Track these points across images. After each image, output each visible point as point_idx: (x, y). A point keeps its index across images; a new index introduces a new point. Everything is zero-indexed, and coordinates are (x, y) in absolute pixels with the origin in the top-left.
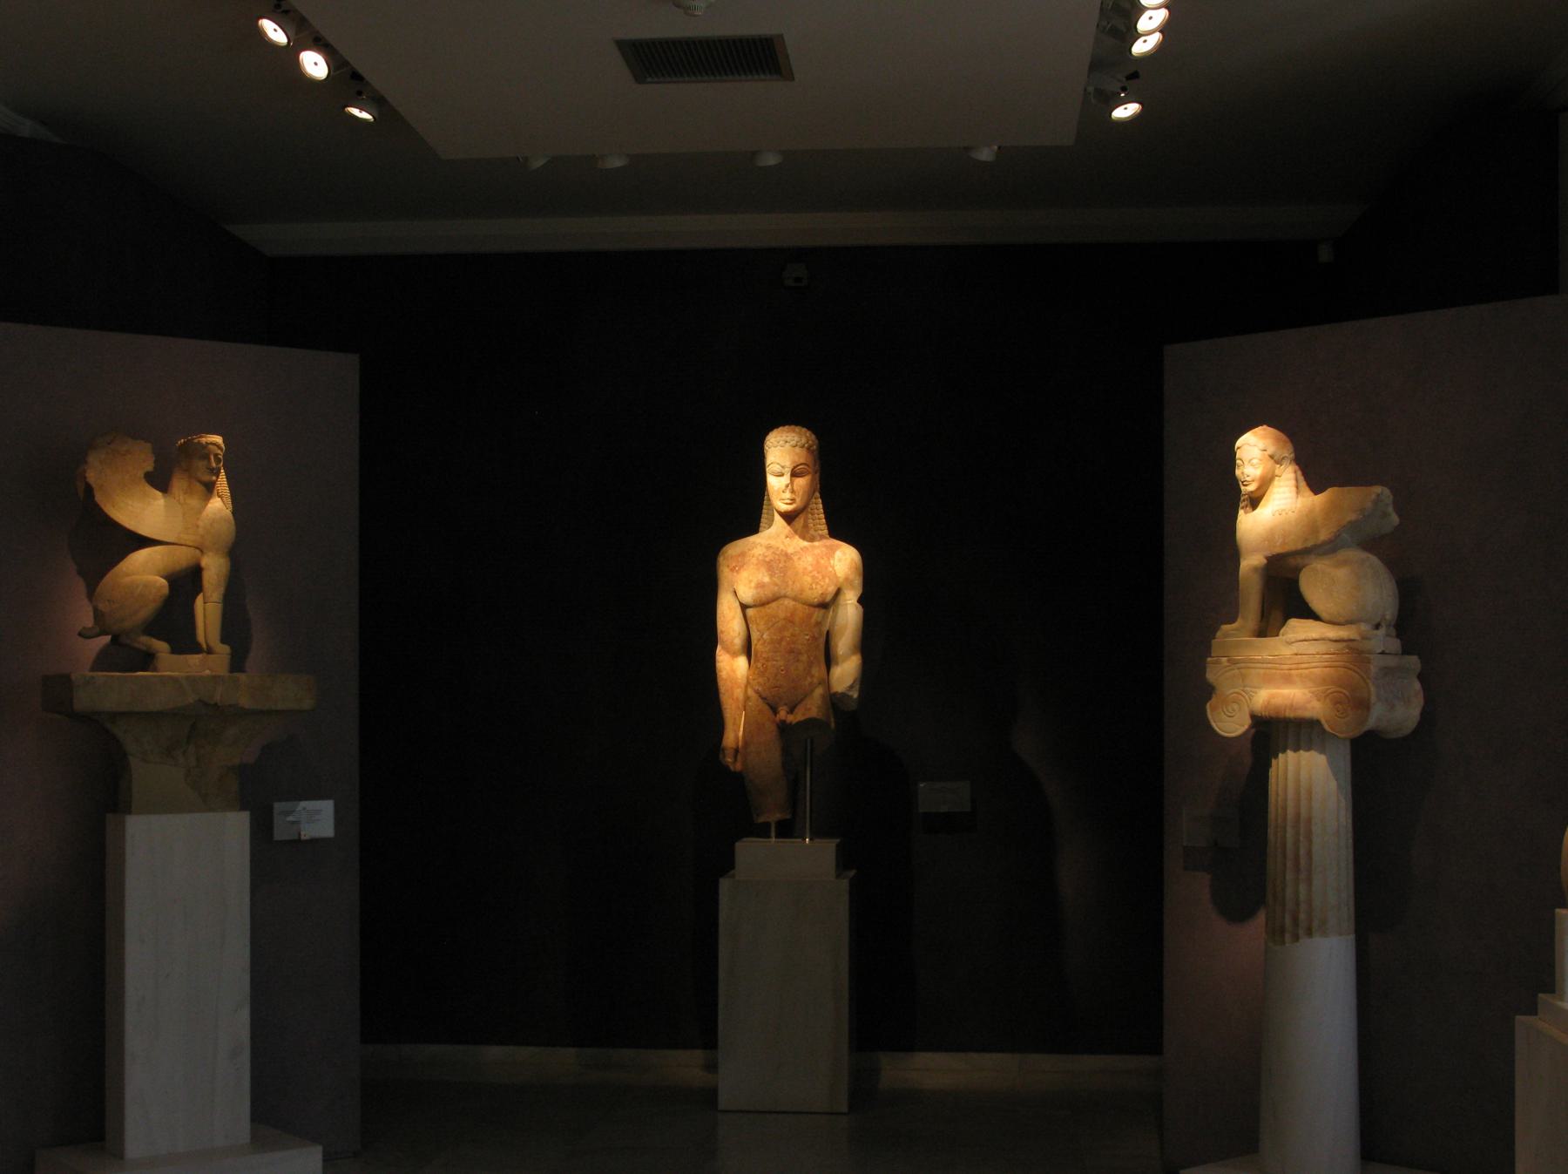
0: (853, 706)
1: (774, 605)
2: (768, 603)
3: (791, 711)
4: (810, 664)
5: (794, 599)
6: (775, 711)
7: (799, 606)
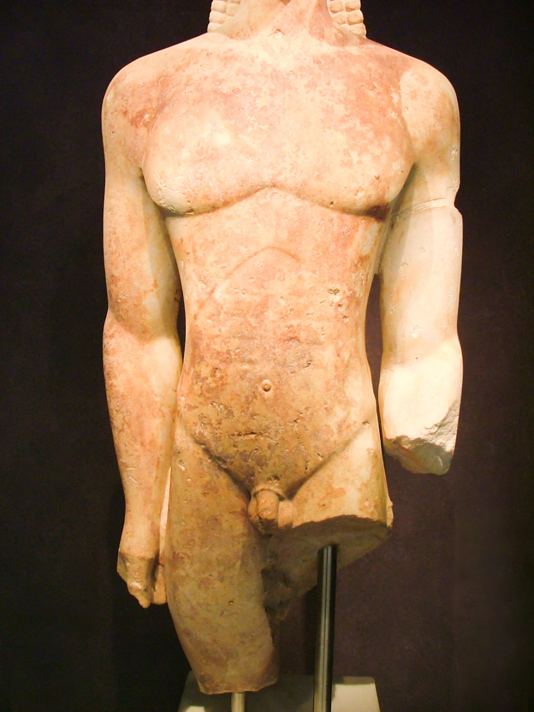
0: (440, 467)
1: (243, 208)
2: (227, 204)
3: (290, 493)
4: (343, 372)
5: (300, 193)
6: (246, 489)
7: (315, 213)
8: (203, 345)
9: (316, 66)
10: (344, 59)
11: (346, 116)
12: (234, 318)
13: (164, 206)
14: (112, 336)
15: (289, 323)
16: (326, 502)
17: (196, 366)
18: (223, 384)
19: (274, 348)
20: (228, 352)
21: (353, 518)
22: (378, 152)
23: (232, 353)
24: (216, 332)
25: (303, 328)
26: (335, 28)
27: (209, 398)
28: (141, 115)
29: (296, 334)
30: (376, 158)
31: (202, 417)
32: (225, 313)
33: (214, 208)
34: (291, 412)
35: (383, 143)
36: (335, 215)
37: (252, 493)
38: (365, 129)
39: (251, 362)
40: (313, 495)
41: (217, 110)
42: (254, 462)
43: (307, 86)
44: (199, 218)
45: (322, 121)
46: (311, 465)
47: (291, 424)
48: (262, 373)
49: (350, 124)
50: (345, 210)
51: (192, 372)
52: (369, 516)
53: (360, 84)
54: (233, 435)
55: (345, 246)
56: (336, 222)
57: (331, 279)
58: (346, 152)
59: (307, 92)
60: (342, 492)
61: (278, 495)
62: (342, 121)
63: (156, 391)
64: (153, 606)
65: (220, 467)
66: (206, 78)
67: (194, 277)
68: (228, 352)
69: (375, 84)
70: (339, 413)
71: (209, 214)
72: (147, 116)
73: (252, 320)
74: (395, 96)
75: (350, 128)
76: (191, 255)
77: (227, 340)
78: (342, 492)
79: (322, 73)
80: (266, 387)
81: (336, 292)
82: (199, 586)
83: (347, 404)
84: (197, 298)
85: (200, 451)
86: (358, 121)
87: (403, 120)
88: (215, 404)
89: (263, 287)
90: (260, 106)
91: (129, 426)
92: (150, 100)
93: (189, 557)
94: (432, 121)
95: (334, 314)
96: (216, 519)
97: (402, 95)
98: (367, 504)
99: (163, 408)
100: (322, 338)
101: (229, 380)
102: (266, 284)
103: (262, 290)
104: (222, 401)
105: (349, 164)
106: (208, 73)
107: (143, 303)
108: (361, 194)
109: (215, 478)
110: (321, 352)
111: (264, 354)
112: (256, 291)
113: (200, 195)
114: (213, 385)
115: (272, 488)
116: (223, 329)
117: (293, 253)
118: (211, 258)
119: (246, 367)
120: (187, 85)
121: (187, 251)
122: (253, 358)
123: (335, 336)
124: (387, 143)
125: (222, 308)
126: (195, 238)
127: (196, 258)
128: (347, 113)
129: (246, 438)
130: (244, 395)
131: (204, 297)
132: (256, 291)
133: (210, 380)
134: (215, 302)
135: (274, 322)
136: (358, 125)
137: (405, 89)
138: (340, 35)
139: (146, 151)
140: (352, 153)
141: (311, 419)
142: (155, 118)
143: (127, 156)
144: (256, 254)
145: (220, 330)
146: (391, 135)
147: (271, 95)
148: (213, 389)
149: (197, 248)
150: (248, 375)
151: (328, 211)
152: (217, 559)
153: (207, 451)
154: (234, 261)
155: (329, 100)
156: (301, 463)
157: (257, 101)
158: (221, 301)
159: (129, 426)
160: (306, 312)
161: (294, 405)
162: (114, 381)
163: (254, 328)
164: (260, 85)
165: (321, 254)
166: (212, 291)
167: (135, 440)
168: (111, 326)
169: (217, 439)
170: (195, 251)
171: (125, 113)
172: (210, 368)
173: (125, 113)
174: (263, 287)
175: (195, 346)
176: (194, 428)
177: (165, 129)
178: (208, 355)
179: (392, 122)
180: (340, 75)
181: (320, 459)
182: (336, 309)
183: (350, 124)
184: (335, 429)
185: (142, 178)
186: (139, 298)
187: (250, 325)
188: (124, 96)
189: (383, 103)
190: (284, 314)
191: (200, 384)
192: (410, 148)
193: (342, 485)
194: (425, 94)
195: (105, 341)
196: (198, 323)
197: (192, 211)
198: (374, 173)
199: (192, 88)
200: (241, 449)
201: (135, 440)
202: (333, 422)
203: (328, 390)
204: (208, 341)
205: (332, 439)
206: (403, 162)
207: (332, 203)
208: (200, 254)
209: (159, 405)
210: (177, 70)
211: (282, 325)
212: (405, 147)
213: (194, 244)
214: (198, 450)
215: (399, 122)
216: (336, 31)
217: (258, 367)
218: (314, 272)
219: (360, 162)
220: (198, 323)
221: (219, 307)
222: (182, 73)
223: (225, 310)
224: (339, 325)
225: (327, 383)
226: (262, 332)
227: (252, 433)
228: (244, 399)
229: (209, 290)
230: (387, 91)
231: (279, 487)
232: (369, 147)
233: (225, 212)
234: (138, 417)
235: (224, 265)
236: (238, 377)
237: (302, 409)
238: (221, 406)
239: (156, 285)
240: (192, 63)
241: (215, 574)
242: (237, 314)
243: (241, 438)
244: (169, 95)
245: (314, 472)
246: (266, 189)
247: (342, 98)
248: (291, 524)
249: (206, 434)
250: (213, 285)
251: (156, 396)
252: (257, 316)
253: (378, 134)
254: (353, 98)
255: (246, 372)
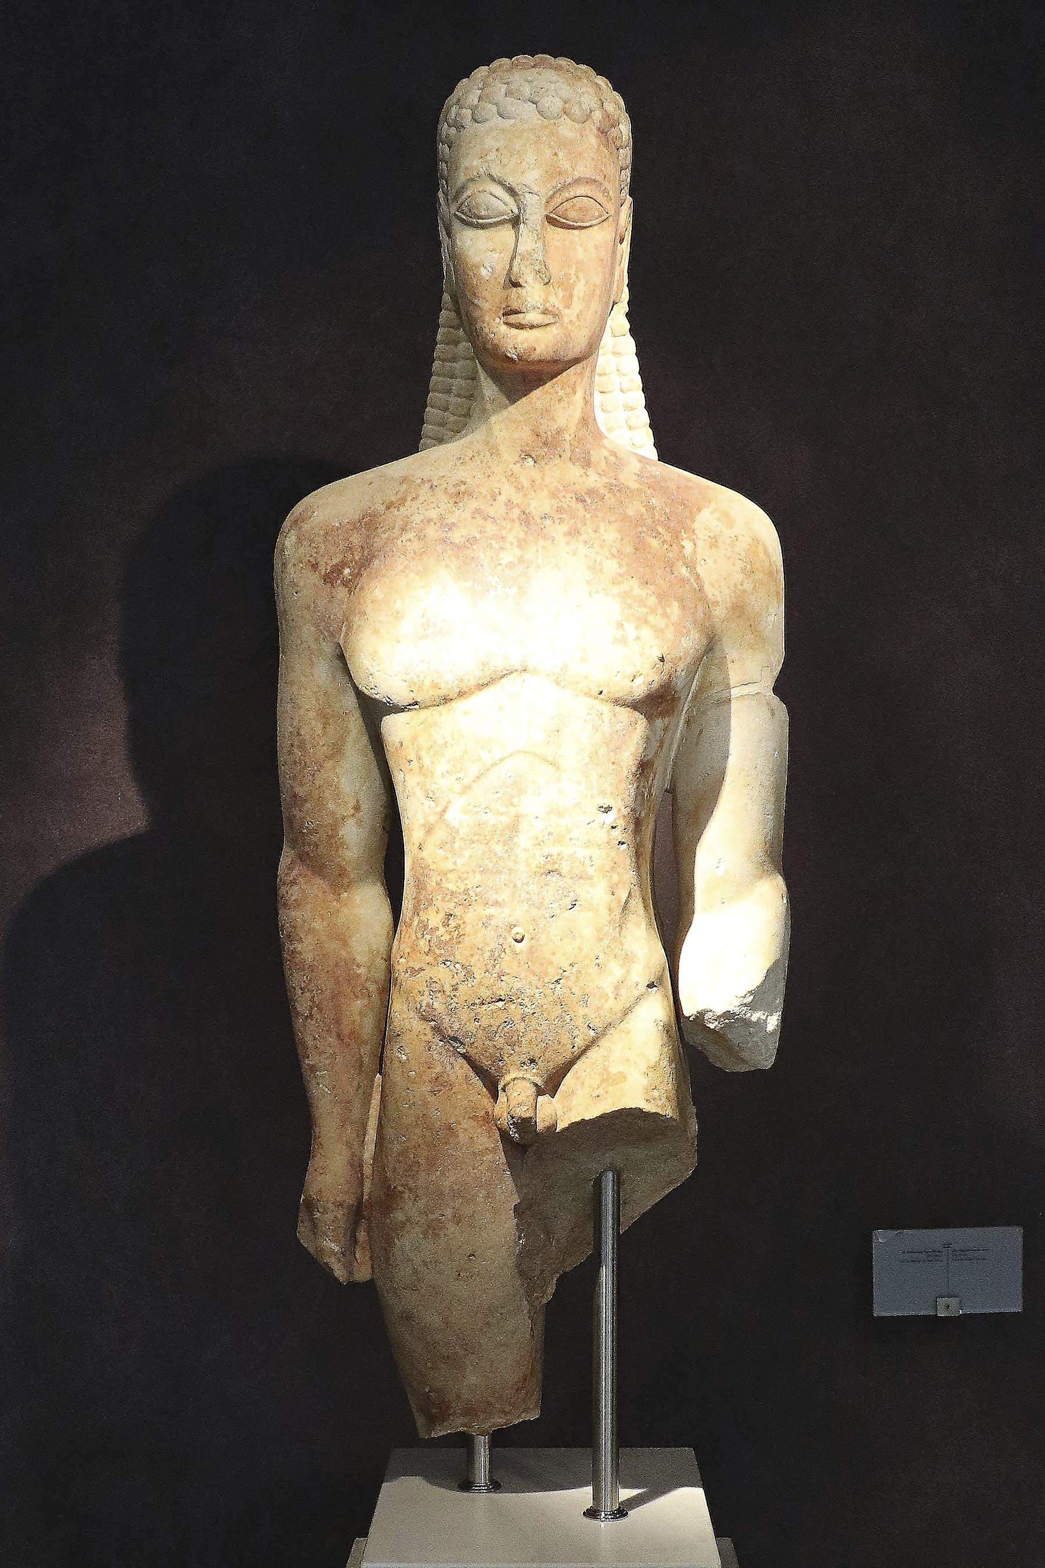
3: (551, 1085)
8: (431, 884)
9: (580, 506)
10: (618, 495)
11: (620, 575)
12: (474, 845)
13: (377, 697)
14: (293, 883)
15: (546, 852)
16: (601, 1091)
17: (421, 914)
18: (459, 936)
19: (527, 884)
20: (466, 891)
21: (636, 1114)
22: (661, 622)
23: (471, 893)
24: (449, 865)
25: (565, 857)
26: (605, 448)
27: (441, 955)
28: (338, 569)
29: (556, 866)
30: (659, 632)
31: (431, 982)
32: (461, 839)
33: (446, 700)
34: (551, 970)
35: (668, 610)
36: (606, 708)
37: (500, 1087)
38: (643, 593)
39: (496, 903)
40: (583, 1084)
41: (447, 566)
42: (502, 1040)
43: (569, 533)
44: (424, 714)
45: (588, 582)
46: (579, 1042)
47: (553, 986)
48: (513, 920)
49: (625, 587)
50: (617, 702)
51: (416, 923)
52: (659, 1111)
53: (640, 529)
54: (474, 1004)
55: (617, 749)
56: (606, 717)
57: (603, 793)
58: (620, 625)
59: (568, 543)
60: (622, 1077)
61: (536, 1085)
62: (615, 582)
63: (359, 959)
64: (353, 1285)
65: (456, 1053)
66: (430, 521)
67: (419, 793)
68: (466, 891)
69: (660, 530)
70: (616, 970)
71: (440, 708)
72: (347, 571)
73: (498, 849)
74: (688, 546)
75: (625, 592)
76: (415, 763)
77: (465, 875)
78: (622, 1077)
79: (588, 516)
80: (519, 937)
81: (608, 809)
82: (425, 1234)
83: (628, 959)
84: (422, 821)
85: (428, 1031)
86: (635, 583)
87: (698, 577)
88: (448, 963)
89: (512, 804)
90: (504, 562)
91: (320, 1010)
92: (350, 549)
93: (410, 1189)
94: (739, 577)
95: (605, 839)
96: (450, 1129)
97: (699, 543)
98: (656, 1093)
99: (368, 984)
100: (591, 871)
101: (468, 929)
102: (515, 801)
103: (511, 808)
104: (458, 958)
105: (624, 641)
106: (433, 514)
107: (341, 833)
108: (639, 681)
109: (449, 1067)
110: (589, 889)
111: (514, 893)
112: (503, 809)
113: (427, 683)
114: (446, 937)
115: (528, 1076)
116: (459, 862)
117: (550, 758)
118: (442, 766)
119: (491, 911)
120: (403, 529)
121: (409, 758)
122: (500, 899)
123: (607, 868)
124: (675, 610)
125: (457, 832)
126: (421, 740)
127: (421, 768)
128: (621, 571)
129: (492, 1007)
130: (488, 949)
131: (432, 819)
132: (503, 809)
133: (442, 930)
134: (448, 826)
135: (527, 850)
136: (636, 587)
137: (702, 535)
138: (612, 458)
139: (347, 620)
140: (625, 623)
141: (577, 978)
142: (359, 574)
143: (317, 626)
144: (502, 760)
145: (455, 863)
146: (681, 601)
147: (520, 547)
148: (446, 943)
149: (423, 753)
150: (493, 922)
151: (597, 702)
152: (452, 1190)
153: (437, 1030)
154: (473, 770)
155: (597, 553)
156: (565, 1039)
157: (501, 555)
158: (455, 824)
159: (320, 1010)
160: (570, 836)
161: (554, 959)
162: (299, 947)
163: (500, 858)
164: (504, 533)
165: (588, 760)
166: (444, 811)
167: (329, 1031)
168: (290, 868)
169: (452, 1011)
170: (419, 758)
171: (315, 567)
172: (442, 915)
173: (315, 567)
174: (512, 804)
175: (420, 886)
176: (419, 998)
177: (376, 591)
178: (439, 897)
179: (683, 581)
180: (612, 519)
181: (592, 1033)
182: (608, 832)
183: (625, 587)
184: (610, 991)
185: (341, 657)
186: (335, 827)
187: (496, 854)
188: (312, 541)
189: (670, 554)
190: (540, 839)
191: (428, 937)
192: (708, 616)
193: (621, 1069)
194: (735, 535)
195: (282, 890)
196: (424, 854)
197: (416, 703)
198: (657, 653)
199: (411, 535)
200: (484, 1022)
201: (329, 1031)
202: (607, 983)
203: (601, 940)
204: (439, 879)
205: (607, 1006)
206: (697, 635)
207: (601, 693)
208: (426, 761)
209: (363, 979)
210: (388, 508)
211: (538, 854)
212: (700, 615)
213: (419, 748)
214: (426, 1027)
215: (692, 580)
216: (607, 454)
217: (506, 910)
218: (579, 783)
219: (638, 638)
220: (424, 854)
221: (453, 832)
222: (396, 513)
223: (462, 835)
224: (613, 854)
225: (599, 930)
226: (511, 864)
227: (501, 1000)
228: (489, 954)
229: (439, 809)
230: (677, 537)
231: (537, 1074)
232: (650, 618)
233: (459, 706)
234: (333, 997)
235: (459, 775)
236: (481, 924)
237: (566, 965)
238: (457, 966)
239: (357, 808)
240: (409, 499)
241: (449, 1212)
242: (478, 841)
243: (485, 1007)
244: (378, 543)
245: (584, 1052)
246: (515, 674)
247: (615, 551)
248: (554, 1126)
249: (436, 1005)
250: (444, 803)
251: (358, 966)
252: (505, 844)
253: (663, 598)
254: (629, 549)
255: (490, 917)
